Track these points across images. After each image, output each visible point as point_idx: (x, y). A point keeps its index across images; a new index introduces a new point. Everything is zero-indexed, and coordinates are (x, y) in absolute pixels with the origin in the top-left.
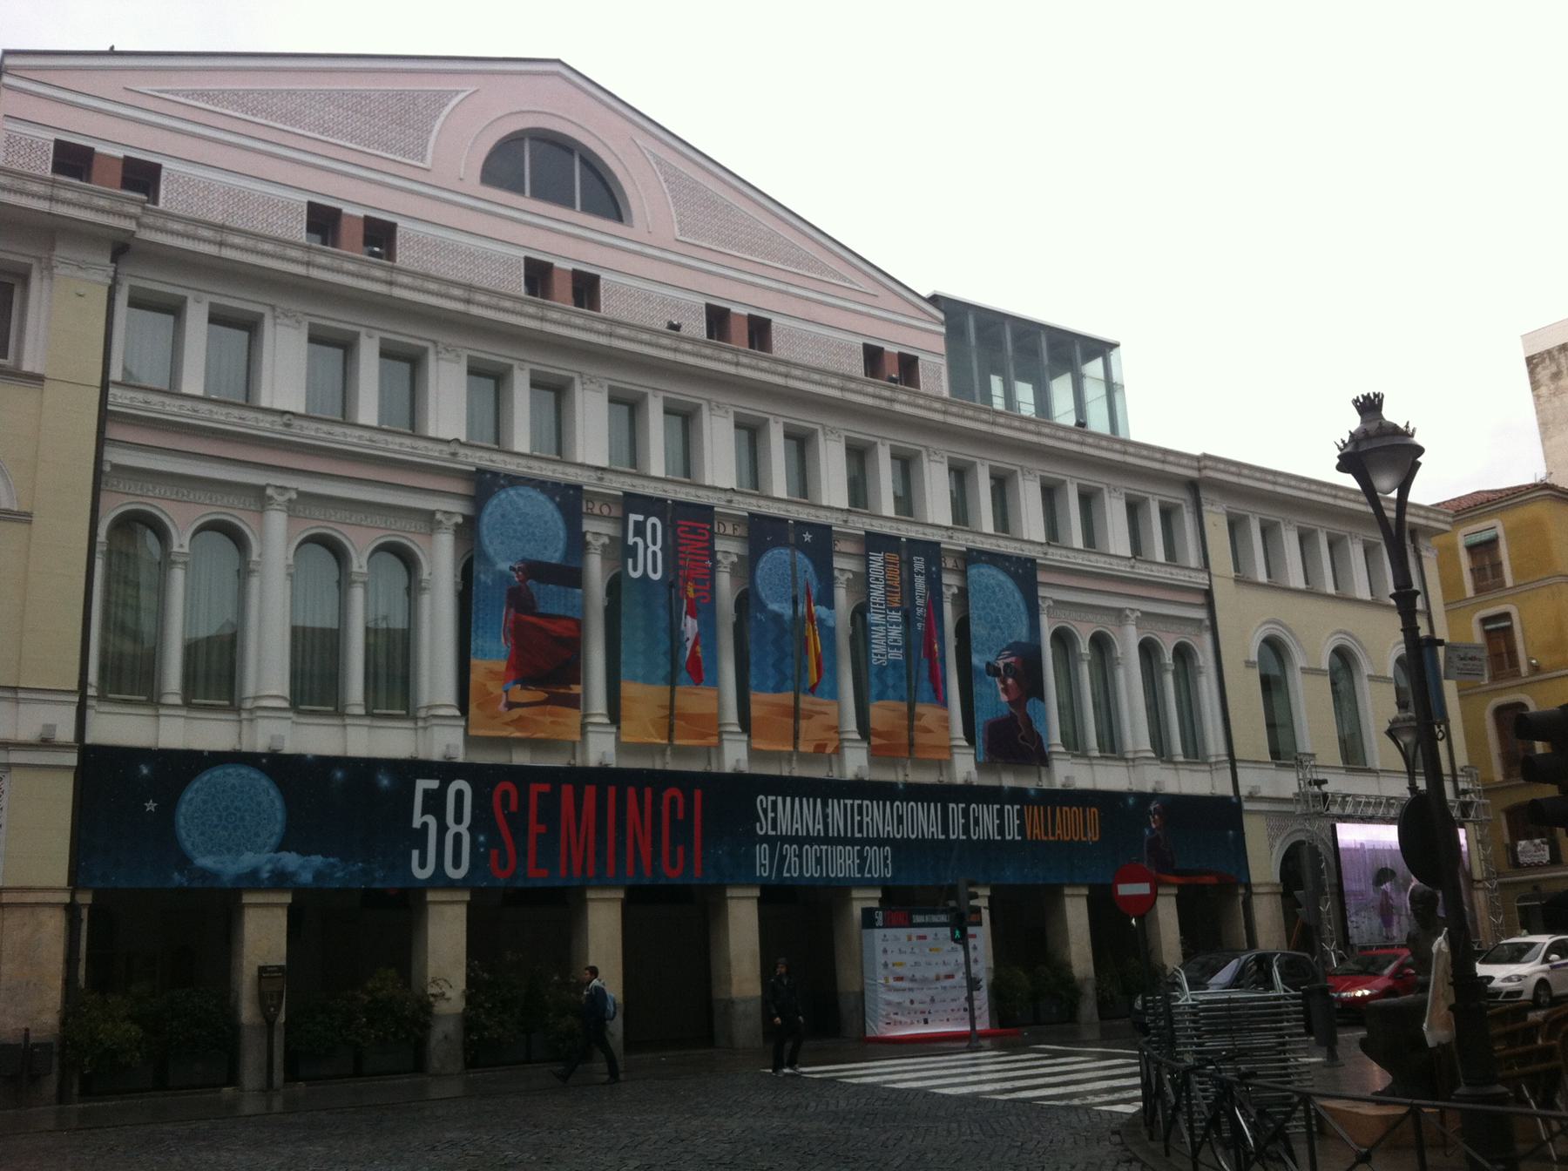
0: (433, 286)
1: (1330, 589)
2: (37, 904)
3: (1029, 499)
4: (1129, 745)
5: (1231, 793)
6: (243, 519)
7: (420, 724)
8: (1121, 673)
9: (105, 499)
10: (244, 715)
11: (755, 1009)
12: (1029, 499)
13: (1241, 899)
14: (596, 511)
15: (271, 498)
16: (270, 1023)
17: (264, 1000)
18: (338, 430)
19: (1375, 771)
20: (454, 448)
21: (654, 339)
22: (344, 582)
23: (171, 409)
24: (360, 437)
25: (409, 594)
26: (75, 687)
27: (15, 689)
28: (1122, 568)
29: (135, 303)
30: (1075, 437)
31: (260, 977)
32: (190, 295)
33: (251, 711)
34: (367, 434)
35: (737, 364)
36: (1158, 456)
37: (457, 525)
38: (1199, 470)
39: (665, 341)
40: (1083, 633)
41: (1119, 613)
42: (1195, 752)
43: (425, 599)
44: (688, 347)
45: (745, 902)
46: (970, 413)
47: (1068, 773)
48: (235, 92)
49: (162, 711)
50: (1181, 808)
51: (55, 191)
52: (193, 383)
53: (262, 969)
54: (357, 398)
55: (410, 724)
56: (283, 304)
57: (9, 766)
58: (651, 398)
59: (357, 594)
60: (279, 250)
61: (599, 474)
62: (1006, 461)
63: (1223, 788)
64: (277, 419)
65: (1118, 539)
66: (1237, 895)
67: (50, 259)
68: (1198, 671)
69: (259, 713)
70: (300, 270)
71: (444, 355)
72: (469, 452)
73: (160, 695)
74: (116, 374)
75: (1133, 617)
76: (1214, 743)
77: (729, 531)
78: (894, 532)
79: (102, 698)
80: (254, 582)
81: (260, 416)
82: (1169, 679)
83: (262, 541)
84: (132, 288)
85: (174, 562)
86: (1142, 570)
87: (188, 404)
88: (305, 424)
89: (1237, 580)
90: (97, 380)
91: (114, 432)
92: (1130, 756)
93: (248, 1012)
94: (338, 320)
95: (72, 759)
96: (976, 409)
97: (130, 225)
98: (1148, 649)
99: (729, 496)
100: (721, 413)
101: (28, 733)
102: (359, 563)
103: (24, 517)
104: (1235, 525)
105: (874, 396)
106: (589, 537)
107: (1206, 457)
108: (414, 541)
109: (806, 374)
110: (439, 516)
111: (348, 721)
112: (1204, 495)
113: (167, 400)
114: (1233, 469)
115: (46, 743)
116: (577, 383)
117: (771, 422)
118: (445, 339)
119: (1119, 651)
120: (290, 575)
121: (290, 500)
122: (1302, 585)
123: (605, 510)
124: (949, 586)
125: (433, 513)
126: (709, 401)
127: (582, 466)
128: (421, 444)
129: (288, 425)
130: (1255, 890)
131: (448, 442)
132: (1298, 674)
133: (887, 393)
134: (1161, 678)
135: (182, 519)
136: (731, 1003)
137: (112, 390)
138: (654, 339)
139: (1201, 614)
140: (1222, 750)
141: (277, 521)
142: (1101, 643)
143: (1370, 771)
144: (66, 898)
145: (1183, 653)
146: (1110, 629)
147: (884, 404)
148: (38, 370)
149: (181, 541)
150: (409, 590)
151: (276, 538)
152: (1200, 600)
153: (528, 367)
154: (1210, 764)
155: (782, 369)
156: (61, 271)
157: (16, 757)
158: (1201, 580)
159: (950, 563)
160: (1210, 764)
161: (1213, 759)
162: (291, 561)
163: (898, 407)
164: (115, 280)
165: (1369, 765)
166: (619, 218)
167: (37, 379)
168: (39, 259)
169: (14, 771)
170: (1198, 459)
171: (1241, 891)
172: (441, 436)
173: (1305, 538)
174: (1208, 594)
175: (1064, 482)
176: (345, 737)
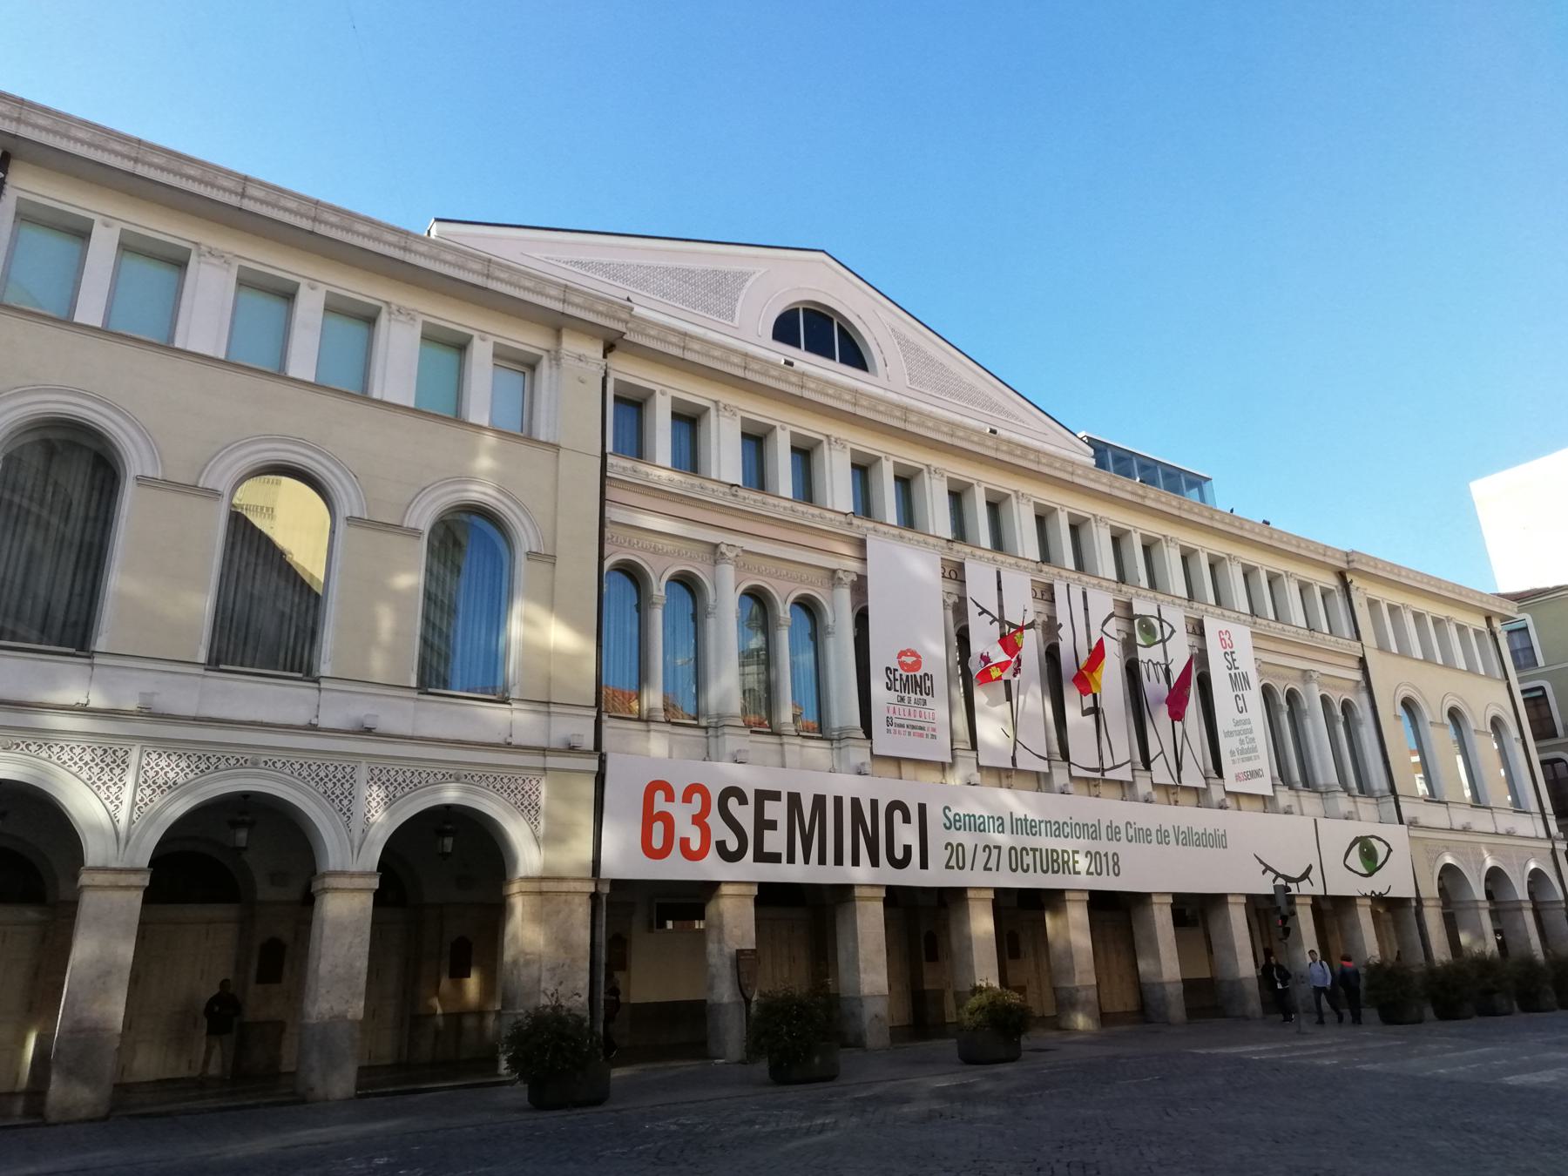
4: (1320, 780)
8: (1308, 723)
9: (608, 549)
10: (711, 732)
26: (593, 703)
28: (1304, 636)
41: (1306, 675)
67: (557, 352)
68: (1359, 722)
74: (609, 448)
76: (1378, 780)
80: (711, 623)
90: (599, 453)
91: (611, 493)
92: (1322, 789)
97: (620, 327)
115: (571, 749)
119: (1305, 704)
130: (1425, 903)
133: (1140, 492)
137: (611, 460)
140: (1385, 786)
141: (728, 572)
142: (1292, 696)
145: (1347, 706)
146: (1299, 687)
147: (1139, 500)
149: (659, 588)
152: (1355, 664)
157: (552, 761)
161: (1378, 794)
170: (1347, 554)
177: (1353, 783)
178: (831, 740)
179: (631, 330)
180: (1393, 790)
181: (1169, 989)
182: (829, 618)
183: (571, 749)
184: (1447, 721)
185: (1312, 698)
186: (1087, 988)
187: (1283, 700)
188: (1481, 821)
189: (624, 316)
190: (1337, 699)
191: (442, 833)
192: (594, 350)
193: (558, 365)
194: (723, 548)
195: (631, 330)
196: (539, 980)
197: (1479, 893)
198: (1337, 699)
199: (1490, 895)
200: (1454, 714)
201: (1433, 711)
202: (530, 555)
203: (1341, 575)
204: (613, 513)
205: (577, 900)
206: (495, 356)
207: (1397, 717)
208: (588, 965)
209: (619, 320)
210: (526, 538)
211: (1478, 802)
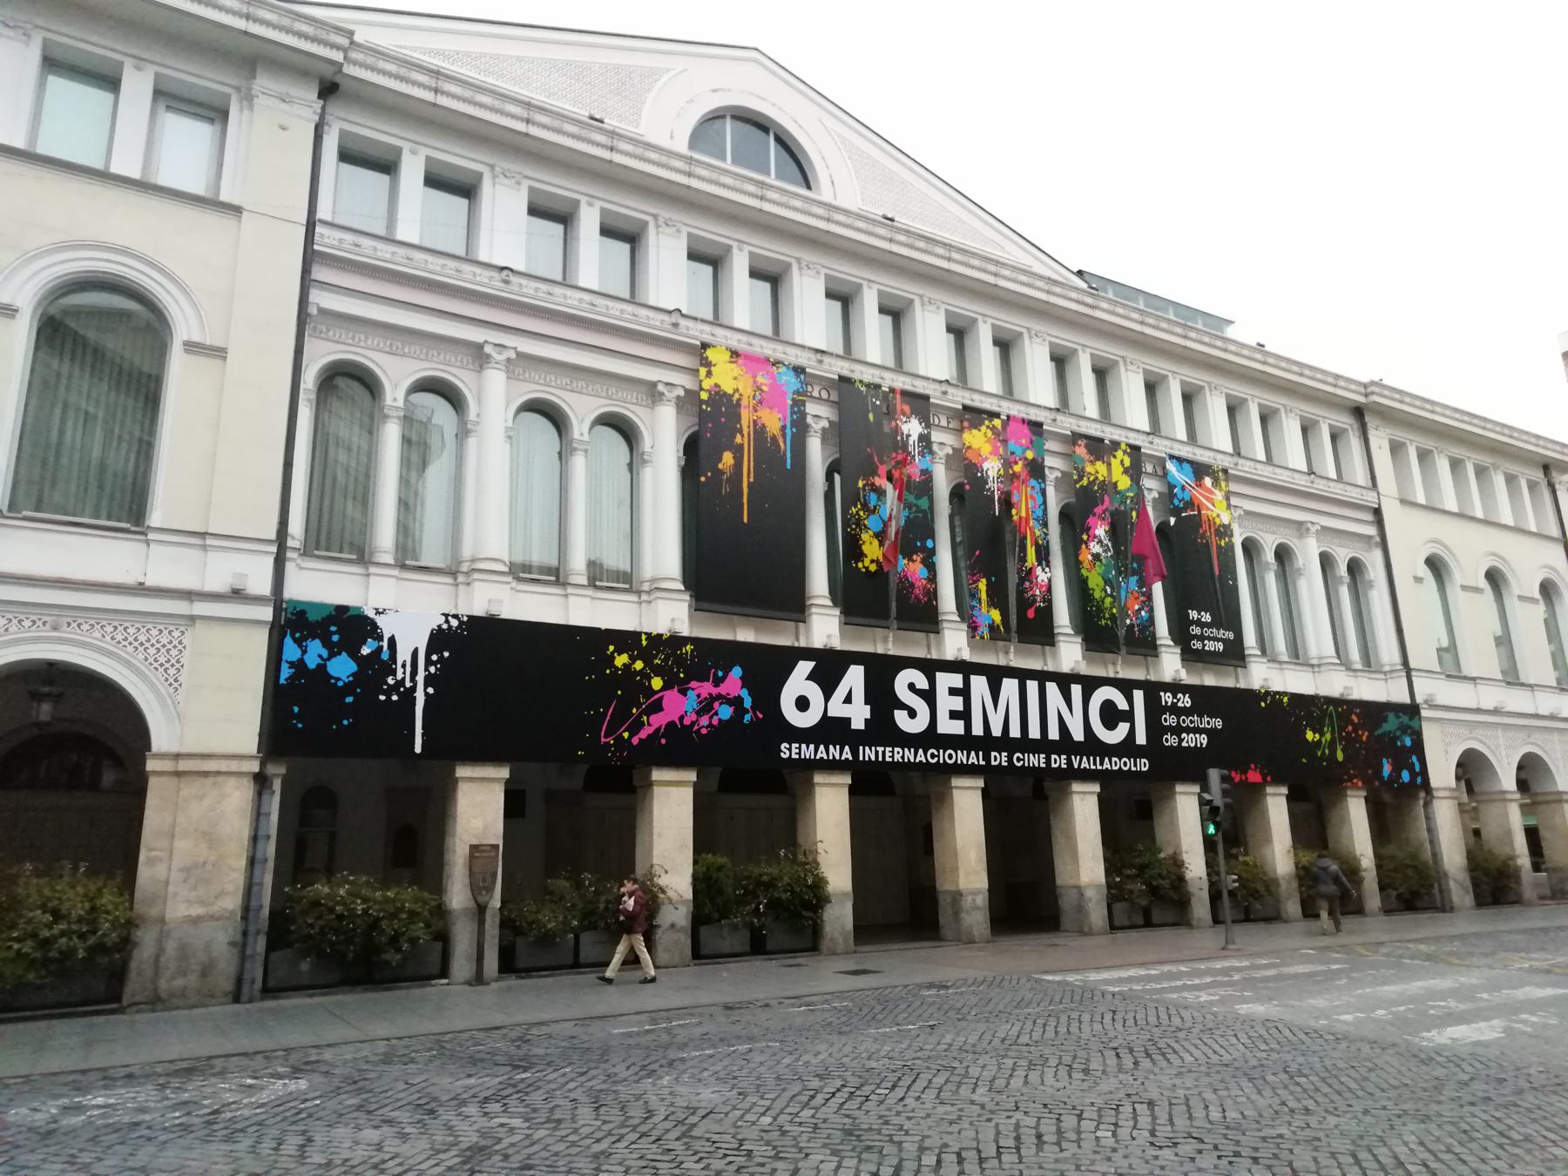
0: (653, 156)
1: (1480, 514)
2: (218, 773)
3: (1215, 410)
5: (1408, 701)
6: (460, 377)
7: (644, 597)
8: (1302, 585)
9: (310, 345)
10: (461, 578)
11: (982, 900)
12: (1215, 410)
13: (1421, 802)
14: (815, 394)
15: (488, 356)
16: (481, 909)
17: (479, 886)
18: (558, 290)
19: (1531, 686)
20: (675, 318)
21: (870, 228)
22: (563, 456)
23: (384, 255)
24: (580, 300)
25: (631, 471)
26: (273, 536)
27: (203, 535)
28: (1302, 482)
29: (346, 156)
30: (1258, 356)
31: (472, 857)
32: (406, 147)
33: (467, 574)
34: (587, 297)
35: (949, 259)
36: (1330, 380)
37: (678, 397)
38: (1366, 395)
39: (881, 231)
40: (1269, 543)
42: (1369, 661)
43: (647, 474)
44: (902, 238)
45: (969, 792)
46: (1164, 325)
47: (1260, 675)
48: (468, 54)
49: (372, 570)
50: (1374, 712)
51: (251, 9)
52: (407, 230)
53: (474, 848)
54: (577, 260)
55: (633, 598)
56: (503, 164)
57: (192, 619)
58: (866, 290)
59: (579, 463)
60: (497, 104)
61: (819, 356)
62: (1196, 377)
63: (1399, 695)
64: (495, 274)
65: (1297, 459)
66: (1417, 799)
67: (250, 89)
68: (1370, 585)
69: (476, 576)
70: (520, 127)
71: (663, 229)
72: (690, 323)
73: (371, 554)
74: (323, 212)
75: (1313, 529)
76: (1388, 652)
77: (944, 423)
78: (1098, 434)
79: (306, 552)
80: (472, 442)
81: (478, 270)
82: (1344, 593)
83: (479, 402)
84: (343, 134)
85: (386, 417)
86: (1320, 487)
87: (402, 251)
88: (524, 281)
89: (1404, 502)
91: (320, 273)
92: (1315, 662)
93: (458, 895)
94: (559, 186)
95: (267, 613)
96: (1169, 321)
97: (338, 56)
98: (1326, 561)
99: (944, 387)
100: (932, 308)
101: (217, 582)
102: (580, 428)
103: (219, 353)
104: (1396, 448)
105: (1078, 302)
106: (809, 420)
107: (1373, 383)
108: (637, 413)
109: (1014, 275)
110: (661, 388)
111: (570, 590)
112: (1367, 419)
113: (380, 245)
114: (1397, 396)
115: (237, 595)
116: (795, 267)
117: (980, 323)
118: (665, 213)
119: (1300, 561)
120: (510, 437)
121: (509, 360)
122: (1455, 509)
123: (824, 395)
124: (1150, 490)
125: (654, 385)
126: (921, 297)
127: (802, 347)
128: (643, 312)
129: (506, 282)
131: (670, 312)
132: (1458, 589)
133: (1089, 300)
134: (1337, 592)
135: (397, 374)
136: (957, 896)
137: (318, 229)
138: (870, 228)
139: (1371, 531)
140: (1396, 658)
142: (1283, 554)
143: (1523, 685)
144: (255, 767)
145: (1355, 567)
148: (236, 202)
149: (394, 394)
150: (630, 466)
151: (494, 397)
152: (1370, 517)
153: (747, 248)
154: (1385, 673)
155: (992, 268)
156: (261, 101)
157: (200, 608)
158: (1370, 498)
159: (1149, 468)
160: (1385, 673)
161: (1387, 668)
162: (510, 424)
163: (1098, 314)
164: (322, 116)
165: (1523, 679)
166: (809, 187)
167: (236, 210)
168: (238, 89)
169: (198, 624)
170: (1365, 386)
171: (1422, 794)
172: (661, 305)
173: (1456, 464)
174: (1377, 512)
175: (1246, 400)
176: (567, 608)
177: (1355, 654)
178: (639, 593)
179: (355, 63)
180: (1405, 663)
181: (1089, 893)
182: (647, 444)
183: (237, 595)
184: (1483, 583)
185: (1308, 553)
186: (975, 893)
187: (1269, 556)
188: (1517, 701)
189: (345, 42)
190: (1342, 556)
191: (37, 697)
192: (312, 94)
193: (251, 107)
194: (488, 349)
195: (355, 63)
196: (167, 883)
197: (1508, 781)
198: (1342, 556)
199: (1522, 785)
200: (1495, 578)
201: (1468, 569)
202: (192, 347)
203: (1358, 412)
204: (319, 298)
205: (232, 781)
206: (158, 94)
207: (1418, 580)
208: (242, 863)
209: (333, 46)
210: (184, 326)
211: (1511, 678)
